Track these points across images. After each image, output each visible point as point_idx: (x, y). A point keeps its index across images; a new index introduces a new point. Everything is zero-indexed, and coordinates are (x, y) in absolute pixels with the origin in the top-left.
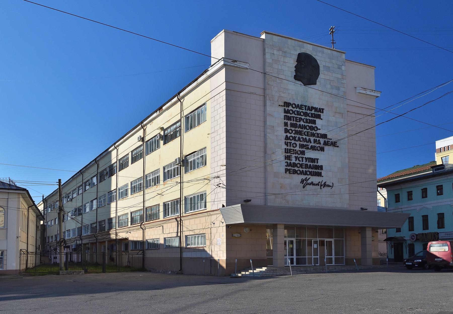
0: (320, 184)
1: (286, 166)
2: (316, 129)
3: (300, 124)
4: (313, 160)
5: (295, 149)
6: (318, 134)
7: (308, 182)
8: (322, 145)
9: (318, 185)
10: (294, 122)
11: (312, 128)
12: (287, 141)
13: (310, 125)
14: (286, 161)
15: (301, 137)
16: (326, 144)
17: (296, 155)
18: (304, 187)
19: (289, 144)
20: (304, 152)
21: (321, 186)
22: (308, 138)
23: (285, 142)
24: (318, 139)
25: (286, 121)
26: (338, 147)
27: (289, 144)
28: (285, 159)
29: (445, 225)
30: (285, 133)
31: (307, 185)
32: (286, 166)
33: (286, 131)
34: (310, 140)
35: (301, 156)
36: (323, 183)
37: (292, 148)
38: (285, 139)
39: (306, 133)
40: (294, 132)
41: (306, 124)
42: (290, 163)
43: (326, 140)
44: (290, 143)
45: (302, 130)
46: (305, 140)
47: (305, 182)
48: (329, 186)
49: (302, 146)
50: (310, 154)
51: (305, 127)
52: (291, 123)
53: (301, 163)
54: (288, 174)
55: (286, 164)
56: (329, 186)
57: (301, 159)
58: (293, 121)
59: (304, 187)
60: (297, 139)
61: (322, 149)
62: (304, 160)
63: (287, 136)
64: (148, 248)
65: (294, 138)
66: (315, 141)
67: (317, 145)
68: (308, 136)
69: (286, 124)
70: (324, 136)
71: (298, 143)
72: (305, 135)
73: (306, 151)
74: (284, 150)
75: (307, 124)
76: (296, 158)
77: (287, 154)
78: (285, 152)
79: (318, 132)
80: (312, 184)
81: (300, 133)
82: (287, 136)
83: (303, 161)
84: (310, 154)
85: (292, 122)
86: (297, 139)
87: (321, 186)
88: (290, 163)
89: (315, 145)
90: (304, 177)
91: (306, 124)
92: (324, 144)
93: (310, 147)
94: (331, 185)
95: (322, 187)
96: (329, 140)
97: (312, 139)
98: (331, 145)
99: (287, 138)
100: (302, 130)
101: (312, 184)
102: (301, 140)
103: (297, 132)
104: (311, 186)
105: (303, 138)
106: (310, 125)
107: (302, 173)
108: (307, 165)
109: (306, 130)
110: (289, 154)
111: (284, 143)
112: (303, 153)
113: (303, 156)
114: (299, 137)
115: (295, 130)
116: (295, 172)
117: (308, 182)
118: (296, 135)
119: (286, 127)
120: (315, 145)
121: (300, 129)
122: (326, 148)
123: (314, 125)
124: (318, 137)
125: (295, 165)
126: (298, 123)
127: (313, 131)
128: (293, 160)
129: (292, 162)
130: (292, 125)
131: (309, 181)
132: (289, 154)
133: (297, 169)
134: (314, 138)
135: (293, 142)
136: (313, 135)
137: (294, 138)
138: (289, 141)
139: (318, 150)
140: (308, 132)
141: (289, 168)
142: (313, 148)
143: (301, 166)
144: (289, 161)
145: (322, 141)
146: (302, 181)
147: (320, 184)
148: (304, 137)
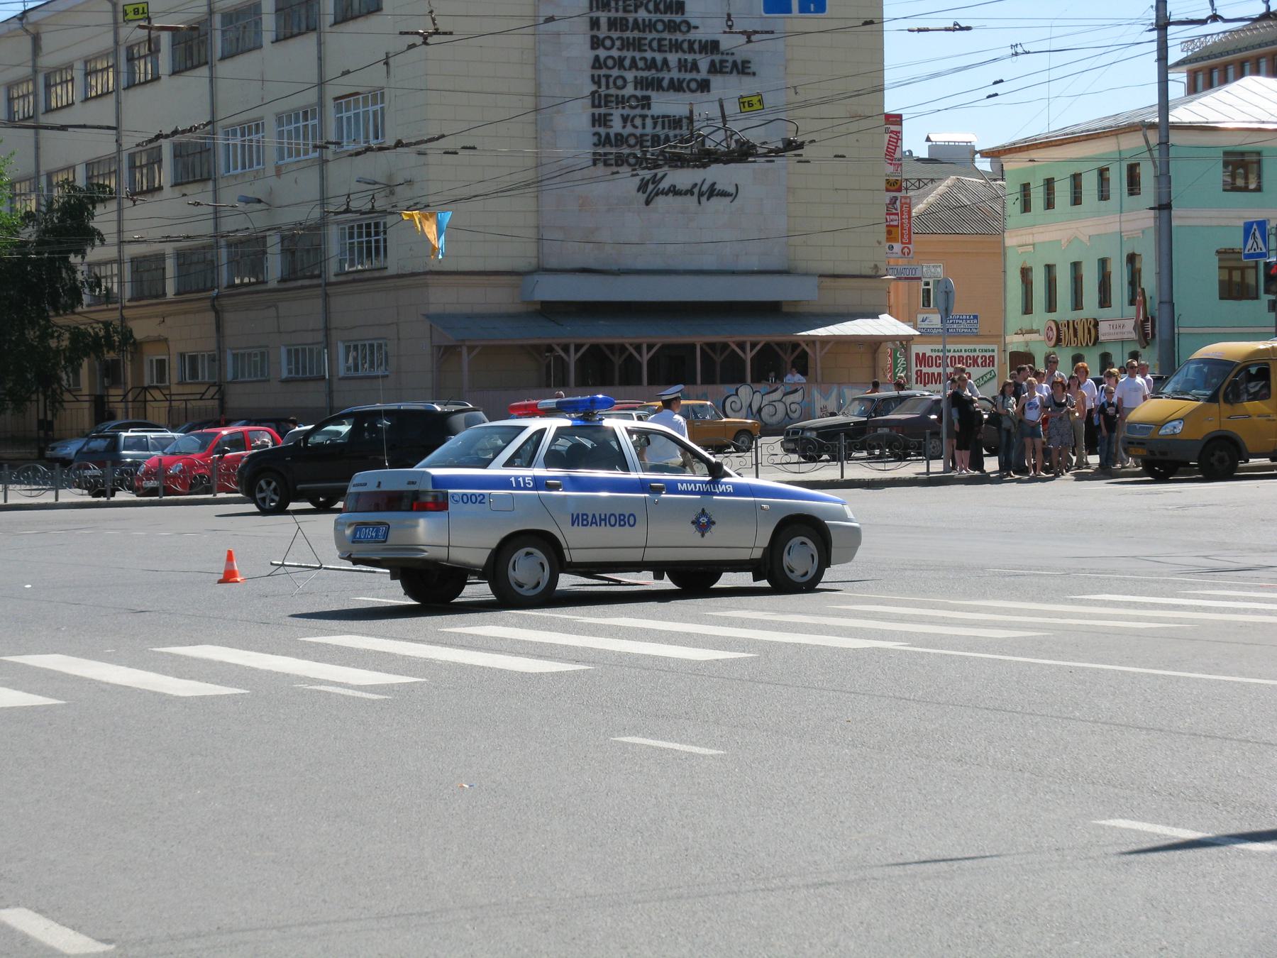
0: (696, 191)
1: (595, 145)
2: (684, 28)
3: (636, 20)
4: (676, 122)
5: (620, 93)
6: (691, 43)
7: (661, 186)
8: (703, 74)
9: (692, 194)
10: (620, 14)
11: (672, 27)
12: (597, 72)
13: (667, 17)
14: (597, 129)
15: (638, 55)
16: (714, 69)
17: (627, 111)
18: (648, 203)
19: (603, 81)
20: (648, 98)
21: (701, 194)
22: (659, 57)
23: (593, 76)
24: (690, 57)
25: (595, 15)
26: (754, 74)
27: (603, 81)
28: (594, 125)
29: (1217, 287)
30: (593, 48)
31: (657, 194)
32: (595, 145)
33: (596, 43)
34: (665, 62)
35: (638, 111)
36: (705, 188)
37: (613, 91)
38: (593, 67)
39: (655, 44)
40: (618, 43)
41: (654, 17)
42: (608, 135)
43: (717, 58)
44: (608, 77)
45: (641, 35)
46: (652, 65)
47: (651, 187)
48: (724, 194)
49: (639, 83)
50: (667, 104)
51: (651, 26)
52: (609, 19)
53: (638, 132)
54: (601, 170)
55: (595, 139)
56: (724, 194)
57: (638, 122)
58: (617, 10)
59: (648, 203)
60: (627, 63)
61: (704, 86)
62: (649, 122)
63: (597, 58)
64: (235, 377)
65: (620, 63)
66: (682, 65)
67: (688, 76)
68: (660, 51)
69: (595, 24)
70: (713, 46)
71: (630, 76)
72: (653, 50)
73: (653, 94)
74: (588, 101)
75: (659, 16)
76: (625, 119)
77: (597, 111)
78: (594, 106)
79: (693, 35)
80: (674, 191)
81: (637, 45)
82: (597, 58)
83: (644, 127)
84: (667, 104)
85: (613, 14)
86: (627, 63)
87: (701, 194)
88: (608, 135)
89: (683, 75)
90: (647, 174)
91: (654, 17)
92: (710, 72)
93: (665, 83)
94: (733, 190)
95: (704, 199)
96: (725, 57)
97: (673, 58)
98: (731, 72)
99: (597, 64)
100: (641, 35)
101: (674, 191)
102: (641, 64)
103: (626, 44)
104: (670, 197)
105: (644, 59)
106: (667, 17)
107: (640, 162)
108: (658, 136)
109: (654, 35)
110: (603, 110)
111: (589, 81)
112: (646, 102)
113: (646, 112)
114: (633, 59)
115: (621, 38)
116: (620, 161)
117: (661, 186)
118: (625, 53)
119: (595, 32)
120: (683, 75)
121: (636, 34)
122: (716, 81)
123: (678, 18)
124: (691, 50)
125: (620, 140)
126: (631, 17)
127: (680, 37)
128: (617, 126)
129: (612, 132)
130: (612, 24)
131: (665, 185)
132: (603, 110)
133: (626, 151)
134: (680, 55)
135: (615, 72)
136: (676, 46)
137: (620, 63)
138: (604, 72)
139: (692, 91)
140: (660, 40)
141: (601, 151)
142: (676, 86)
143: (640, 140)
144: (602, 131)
145: (704, 62)
146: (643, 187)
147: (696, 191)
148: (649, 55)
